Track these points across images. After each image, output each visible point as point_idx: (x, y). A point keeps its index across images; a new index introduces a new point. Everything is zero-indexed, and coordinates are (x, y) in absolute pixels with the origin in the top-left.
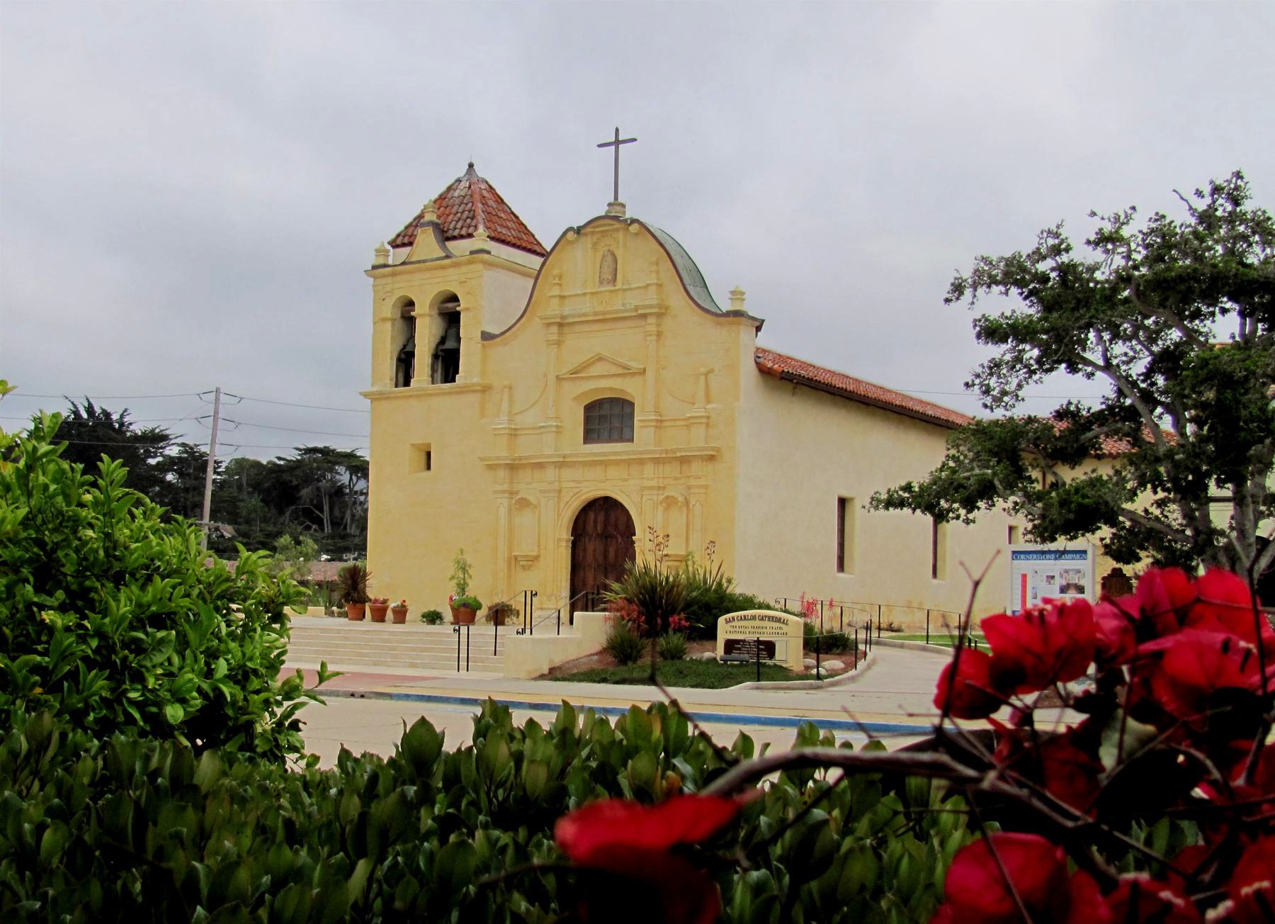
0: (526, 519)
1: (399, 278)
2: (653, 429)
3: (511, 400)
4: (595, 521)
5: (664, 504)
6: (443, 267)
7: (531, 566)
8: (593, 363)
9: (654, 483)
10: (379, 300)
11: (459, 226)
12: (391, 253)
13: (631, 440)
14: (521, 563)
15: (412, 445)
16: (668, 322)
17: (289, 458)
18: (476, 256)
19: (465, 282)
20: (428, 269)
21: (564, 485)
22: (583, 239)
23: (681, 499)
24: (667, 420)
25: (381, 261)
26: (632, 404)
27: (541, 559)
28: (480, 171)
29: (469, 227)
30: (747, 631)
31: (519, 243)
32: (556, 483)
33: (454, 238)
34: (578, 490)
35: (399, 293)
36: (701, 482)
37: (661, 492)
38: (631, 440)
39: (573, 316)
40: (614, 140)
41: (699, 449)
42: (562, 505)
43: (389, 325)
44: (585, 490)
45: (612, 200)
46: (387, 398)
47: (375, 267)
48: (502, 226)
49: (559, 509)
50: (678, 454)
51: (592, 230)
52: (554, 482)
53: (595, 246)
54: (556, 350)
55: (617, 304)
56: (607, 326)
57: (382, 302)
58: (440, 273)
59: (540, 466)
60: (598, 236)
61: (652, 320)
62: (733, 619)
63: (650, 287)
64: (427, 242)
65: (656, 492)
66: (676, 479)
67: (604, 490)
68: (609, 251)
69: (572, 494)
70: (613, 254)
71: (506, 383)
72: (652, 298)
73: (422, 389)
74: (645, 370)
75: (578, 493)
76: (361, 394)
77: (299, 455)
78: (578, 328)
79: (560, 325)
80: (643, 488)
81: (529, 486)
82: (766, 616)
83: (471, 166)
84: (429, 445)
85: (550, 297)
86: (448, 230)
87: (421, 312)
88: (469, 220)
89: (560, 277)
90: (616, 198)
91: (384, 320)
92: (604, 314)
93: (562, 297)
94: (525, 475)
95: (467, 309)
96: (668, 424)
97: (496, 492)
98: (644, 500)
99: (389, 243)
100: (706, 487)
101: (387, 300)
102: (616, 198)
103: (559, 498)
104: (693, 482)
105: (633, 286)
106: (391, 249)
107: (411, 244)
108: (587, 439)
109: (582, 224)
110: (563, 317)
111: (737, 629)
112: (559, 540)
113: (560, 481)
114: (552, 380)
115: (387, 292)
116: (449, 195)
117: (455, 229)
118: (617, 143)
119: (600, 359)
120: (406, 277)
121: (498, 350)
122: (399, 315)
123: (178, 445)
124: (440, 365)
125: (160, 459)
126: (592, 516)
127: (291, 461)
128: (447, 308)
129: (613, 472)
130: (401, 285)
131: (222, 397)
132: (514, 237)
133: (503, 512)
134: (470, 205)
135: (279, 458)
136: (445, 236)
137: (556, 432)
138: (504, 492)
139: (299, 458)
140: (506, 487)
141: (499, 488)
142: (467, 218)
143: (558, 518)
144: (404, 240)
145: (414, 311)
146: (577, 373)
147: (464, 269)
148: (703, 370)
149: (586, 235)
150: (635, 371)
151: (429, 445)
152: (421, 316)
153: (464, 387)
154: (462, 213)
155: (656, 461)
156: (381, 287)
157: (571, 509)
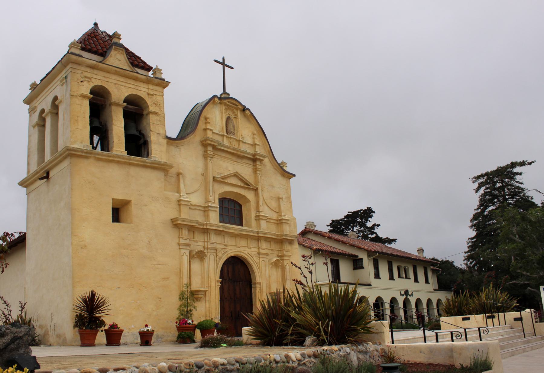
1: (96, 72)
5: (274, 264)
34: (226, 250)
35: (96, 82)
50: (284, 237)
67: (241, 252)
73: (122, 157)
91: (83, 96)
92: (237, 151)
98: (261, 259)
101: (85, 83)
104: (285, 253)
105: (247, 142)
115: (85, 77)
119: (236, 175)
129: (243, 242)
133: (186, 259)
140: (187, 242)
141: (182, 241)
146: (220, 181)
150: (252, 187)
155: (268, 239)
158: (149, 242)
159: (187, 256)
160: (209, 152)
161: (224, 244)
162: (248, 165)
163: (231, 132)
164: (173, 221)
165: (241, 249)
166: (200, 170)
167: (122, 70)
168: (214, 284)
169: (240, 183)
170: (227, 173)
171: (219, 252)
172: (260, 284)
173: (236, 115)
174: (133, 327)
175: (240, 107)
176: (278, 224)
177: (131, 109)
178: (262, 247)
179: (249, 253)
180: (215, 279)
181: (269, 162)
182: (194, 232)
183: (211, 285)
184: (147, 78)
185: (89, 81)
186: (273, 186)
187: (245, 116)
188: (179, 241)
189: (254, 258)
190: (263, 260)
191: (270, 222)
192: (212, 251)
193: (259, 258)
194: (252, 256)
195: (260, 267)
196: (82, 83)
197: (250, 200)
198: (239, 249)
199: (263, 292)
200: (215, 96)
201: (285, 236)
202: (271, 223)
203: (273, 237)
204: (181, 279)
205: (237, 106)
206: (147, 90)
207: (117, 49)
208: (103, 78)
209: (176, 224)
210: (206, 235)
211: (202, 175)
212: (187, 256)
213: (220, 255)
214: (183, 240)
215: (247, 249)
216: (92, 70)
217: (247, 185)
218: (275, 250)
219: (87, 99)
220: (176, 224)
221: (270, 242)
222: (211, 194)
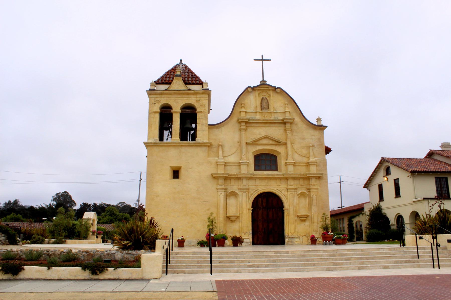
0: (232, 201)
1: (163, 96)
2: (293, 166)
3: (223, 152)
4: (262, 202)
5: (300, 195)
6: (188, 94)
7: (235, 220)
8: (262, 139)
9: (293, 187)
10: (151, 104)
11: (190, 79)
14: (232, 219)
15: (170, 167)
19: (200, 101)
21: (250, 187)
22: (254, 92)
24: (297, 163)
25: (153, 88)
27: (240, 218)
32: (247, 186)
33: (190, 84)
34: (257, 189)
36: (316, 187)
37: (296, 190)
38: (276, 170)
39: (254, 120)
41: (314, 174)
42: (250, 195)
46: (158, 146)
47: (150, 90)
49: (248, 197)
50: (308, 176)
51: (259, 88)
52: (245, 186)
53: (259, 94)
54: (245, 132)
55: (268, 117)
56: (267, 125)
59: (239, 179)
60: (260, 91)
63: (286, 113)
65: (294, 190)
66: (301, 185)
67: (270, 189)
68: (265, 97)
69: (255, 191)
70: (267, 99)
71: (220, 144)
72: (288, 116)
74: (286, 144)
75: (257, 190)
78: (253, 125)
79: (246, 123)
80: (287, 189)
81: (234, 187)
83: (181, 61)
84: (180, 168)
85: (240, 112)
89: (244, 104)
91: (155, 112)
93: (246, 112)
94: (233, 182)
95: (201, 112)
96: (297, 164)
97: (217, 189)
98: (289, 193)
100: (317, 189)
103: (249, 192)
104: (312, 187)
105: (278, 111)
107: (169, 83)
108: (255, 170)
109: (255, 85)
110: (249, 120)
112: (249, 209)
113: (248, 185)
114: (243, 144)
115: (157, 101)
119: (266, 137)
120: (166, 96)
121: (215, 131)
126: (260, 200)
128: (185, 111)
129: (273, 182)
130: (165, 99)
137: (248, 165)
138: (222, 189)
140: (223, 187)
141: (219, 187)
145: (172, 110)
146: (255, 142)
147: (199, 96)
149: (255, 90)
151: (180, 168)
152: (176, 112)
153: (203, 143)
155: (294, 178)
156: (153, 99)
158: (198, 189)
159: (223, 195)
160: (242, 127)
161: (255, 185)
163: (264, 108)
164: (212, 175)
165: (271, 187)
166: (237, 140)
167: (178, 91)
168: (246, 211)
169: (271, 142)
170: (259, 137)
171: (251, 191)
172: (288, 209)
173: (269, 94)
174: (188, 237)
175: (271, 88)
176: (308, 165)
177: (189, 112)
178: (290, 184)
179: (279, 189)
180: (247, 208)
181: (301, 121)
182: (231, 180)
183: (243, 212)
184: (195, 92)
185: (159, 103)
186: (303, 139)
187: (277, 93)
188: (217, 187)
189: (283, 192)
190: (291, 193)
191: (300, 165)
192: (245, 190)
193: (287, 191)
194: (281, 191)
195: (288, 198)
196: (155, 105)
197: (281, 152)
198: (268, 187)
199: (290, 215)
200: (249, 87)
201: (308, 175)
203: (297, 176)
204: (218, 209)
205: (269, 88)
206: (195, 99)
207: (177, 78)
208: (167, 99)
209: (215, 177)
210: (240, 180)
211: (238, 143)
212: (223, 195)
213: (252, 192)
214: (220, 186)
215: (276, 187)
216: (161, 96)
217: (278, 143)
218: (304, 185)
219: (157, 113)
220: (215, 177)
221: (299, 179)
222: (244, 154)
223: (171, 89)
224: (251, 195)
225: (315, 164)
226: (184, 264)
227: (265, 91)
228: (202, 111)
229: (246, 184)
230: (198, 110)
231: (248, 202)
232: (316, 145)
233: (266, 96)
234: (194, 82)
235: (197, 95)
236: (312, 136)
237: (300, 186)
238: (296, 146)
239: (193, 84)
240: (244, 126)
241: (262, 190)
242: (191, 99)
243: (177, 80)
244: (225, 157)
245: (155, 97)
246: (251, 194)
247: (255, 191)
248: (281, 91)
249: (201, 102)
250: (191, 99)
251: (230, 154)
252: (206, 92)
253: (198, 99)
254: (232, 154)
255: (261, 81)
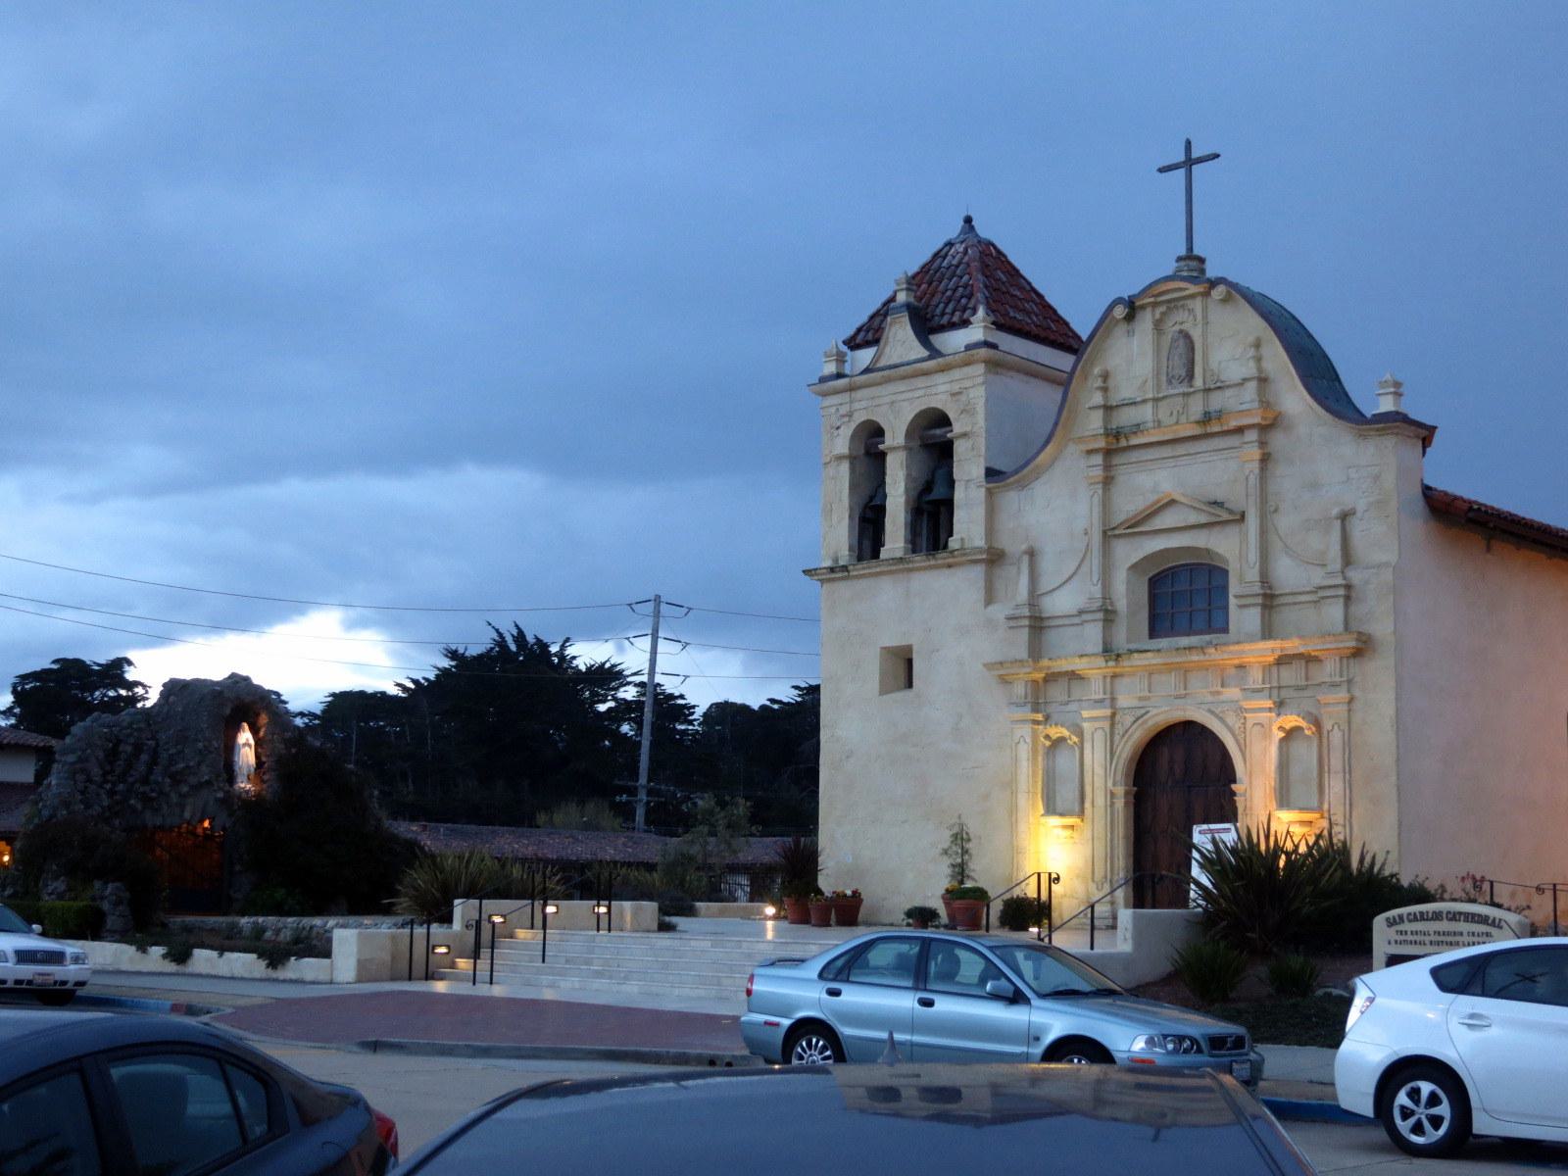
1: (859, 394)
6: (926, 373)
12: (848, 358)
13: (1225, 630)
16: (1278, 440)
17: (786, 700)
18: (974, 352)
20: (903, 378)
23: (1303, 724)
24: (1286, 594)
26: (1225, 572)
28: (984, 231)
29: (964, 310)
30: (1427, 939)
31: (1043, 334)
33: (942, 329)
34: (1143, 711)
35: (860, 417)
40: (1182, 158)
42: (1117, 738)
43: (845, 467)
44: (1154, 711)
45: (1183, 252)
48: (1015, 307)
51: (1152, 300)
56: (1181, 449)
57: (835, 434)
58: (920, 382)
61: (1252, 436)
62: (1401, 917)
64: (902, 341)
70: (1187, 337)
75: (1142, 716)
76: (804, 571)
77: (799, 696)
82: (1460, 913)
83: (968, 220)
84: (909, 649)
85: (1090, 408)
86: (933, 316)
87: (895, 444)
88: (964, 301)
89: (1105, 376)
90: (1190, 248)
91: (840, 458)
95: (964, 435)
98: (1249, 725)
99: (844, 343)
102: (1190, 248)
106: (849, 352)
107: (876, 342)
111: (1410, 938)
115: (843, 416)
116: (936, 265)
117: (943, 314)
118: (1189, 162)
121: (1010, 499)
122: (862, 451)
123: (636, 685)
124: (925, 526)
125: (611, 704)
126: (1165, 754)
127: (789, 704)
128: (934, 436)
130: (864, 404)
131: (663, 607)
132: (1037, 326)
134: (966, 278)
135: (772, 701)
136: (926, 325)
139: (799, 699)
142: (962, 297)
143: (1112, 760)
144: (869, 335)
145: (883, 442)
146: (1136, 526)
147: (957, 374)
148: (1335, 511)
149: (1143, 307)
151: (909, 649)
152: (894, 449)
154: (955, 291)
156: (833, 410)
157: (1130, 743)
162: (1226, 452)
168: (1103, 800)
186: (1314, 486)
189: (1231, 719)
202: (1301, 606)
205: (1181, 289)
218: (1307, 685)
223: (882, 363)
224: (1123, 736)
225: (1337, 596)
226: (693, 973)
227: (1181, 303)
228: (968, 429)
229: (1101, 696)
230: (957, 428)
231: (1112, 760)
232: (1361, 506)
233: (1184, 327)
234: (955, 319)
235: (951, 372)
236: (1350, 467)
237: (1292, 693)
238: (1285, 522)
239: (953, 326)
240: (1096, 466)
241: (1157, 715)
242: (934, 391)
243: (897, 326)
244: (1043, 594)
245: (836, 403)
246: (1121, 733)
247: (1135, 722)
248: (1228, 292)
249: (963, 398)
250: (934, 391)
251: (1057, 585)
252: (972, 355)
253: (956, 388)
254: (1064, 583)
255: (1179, 259)
